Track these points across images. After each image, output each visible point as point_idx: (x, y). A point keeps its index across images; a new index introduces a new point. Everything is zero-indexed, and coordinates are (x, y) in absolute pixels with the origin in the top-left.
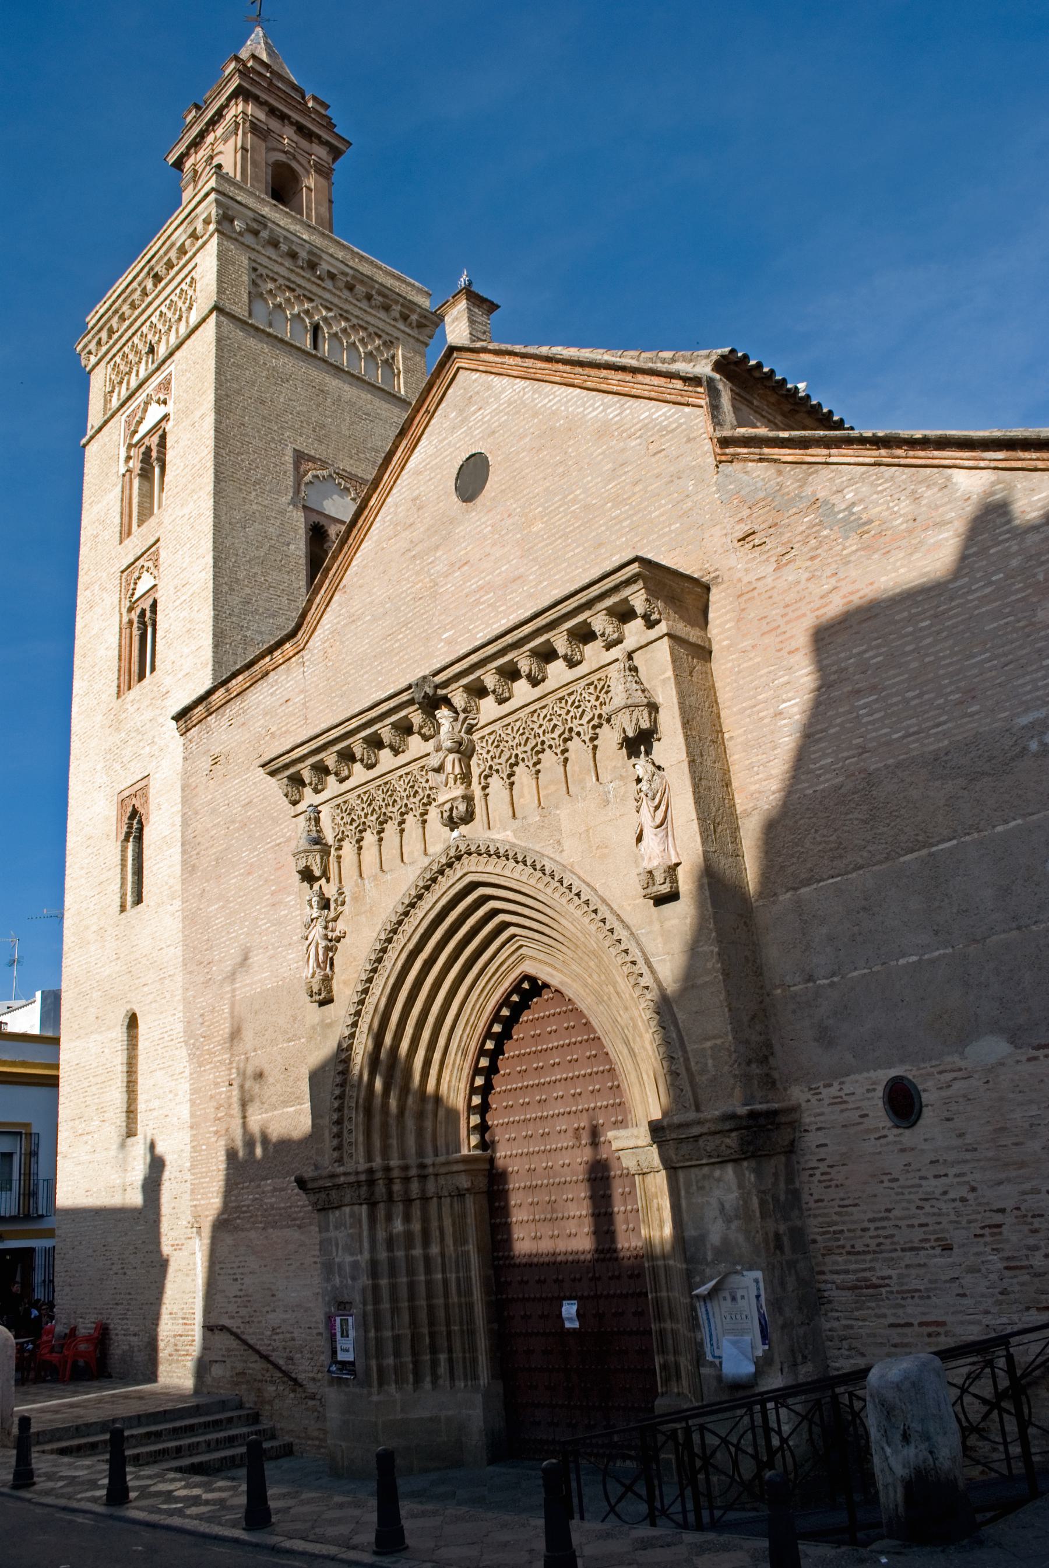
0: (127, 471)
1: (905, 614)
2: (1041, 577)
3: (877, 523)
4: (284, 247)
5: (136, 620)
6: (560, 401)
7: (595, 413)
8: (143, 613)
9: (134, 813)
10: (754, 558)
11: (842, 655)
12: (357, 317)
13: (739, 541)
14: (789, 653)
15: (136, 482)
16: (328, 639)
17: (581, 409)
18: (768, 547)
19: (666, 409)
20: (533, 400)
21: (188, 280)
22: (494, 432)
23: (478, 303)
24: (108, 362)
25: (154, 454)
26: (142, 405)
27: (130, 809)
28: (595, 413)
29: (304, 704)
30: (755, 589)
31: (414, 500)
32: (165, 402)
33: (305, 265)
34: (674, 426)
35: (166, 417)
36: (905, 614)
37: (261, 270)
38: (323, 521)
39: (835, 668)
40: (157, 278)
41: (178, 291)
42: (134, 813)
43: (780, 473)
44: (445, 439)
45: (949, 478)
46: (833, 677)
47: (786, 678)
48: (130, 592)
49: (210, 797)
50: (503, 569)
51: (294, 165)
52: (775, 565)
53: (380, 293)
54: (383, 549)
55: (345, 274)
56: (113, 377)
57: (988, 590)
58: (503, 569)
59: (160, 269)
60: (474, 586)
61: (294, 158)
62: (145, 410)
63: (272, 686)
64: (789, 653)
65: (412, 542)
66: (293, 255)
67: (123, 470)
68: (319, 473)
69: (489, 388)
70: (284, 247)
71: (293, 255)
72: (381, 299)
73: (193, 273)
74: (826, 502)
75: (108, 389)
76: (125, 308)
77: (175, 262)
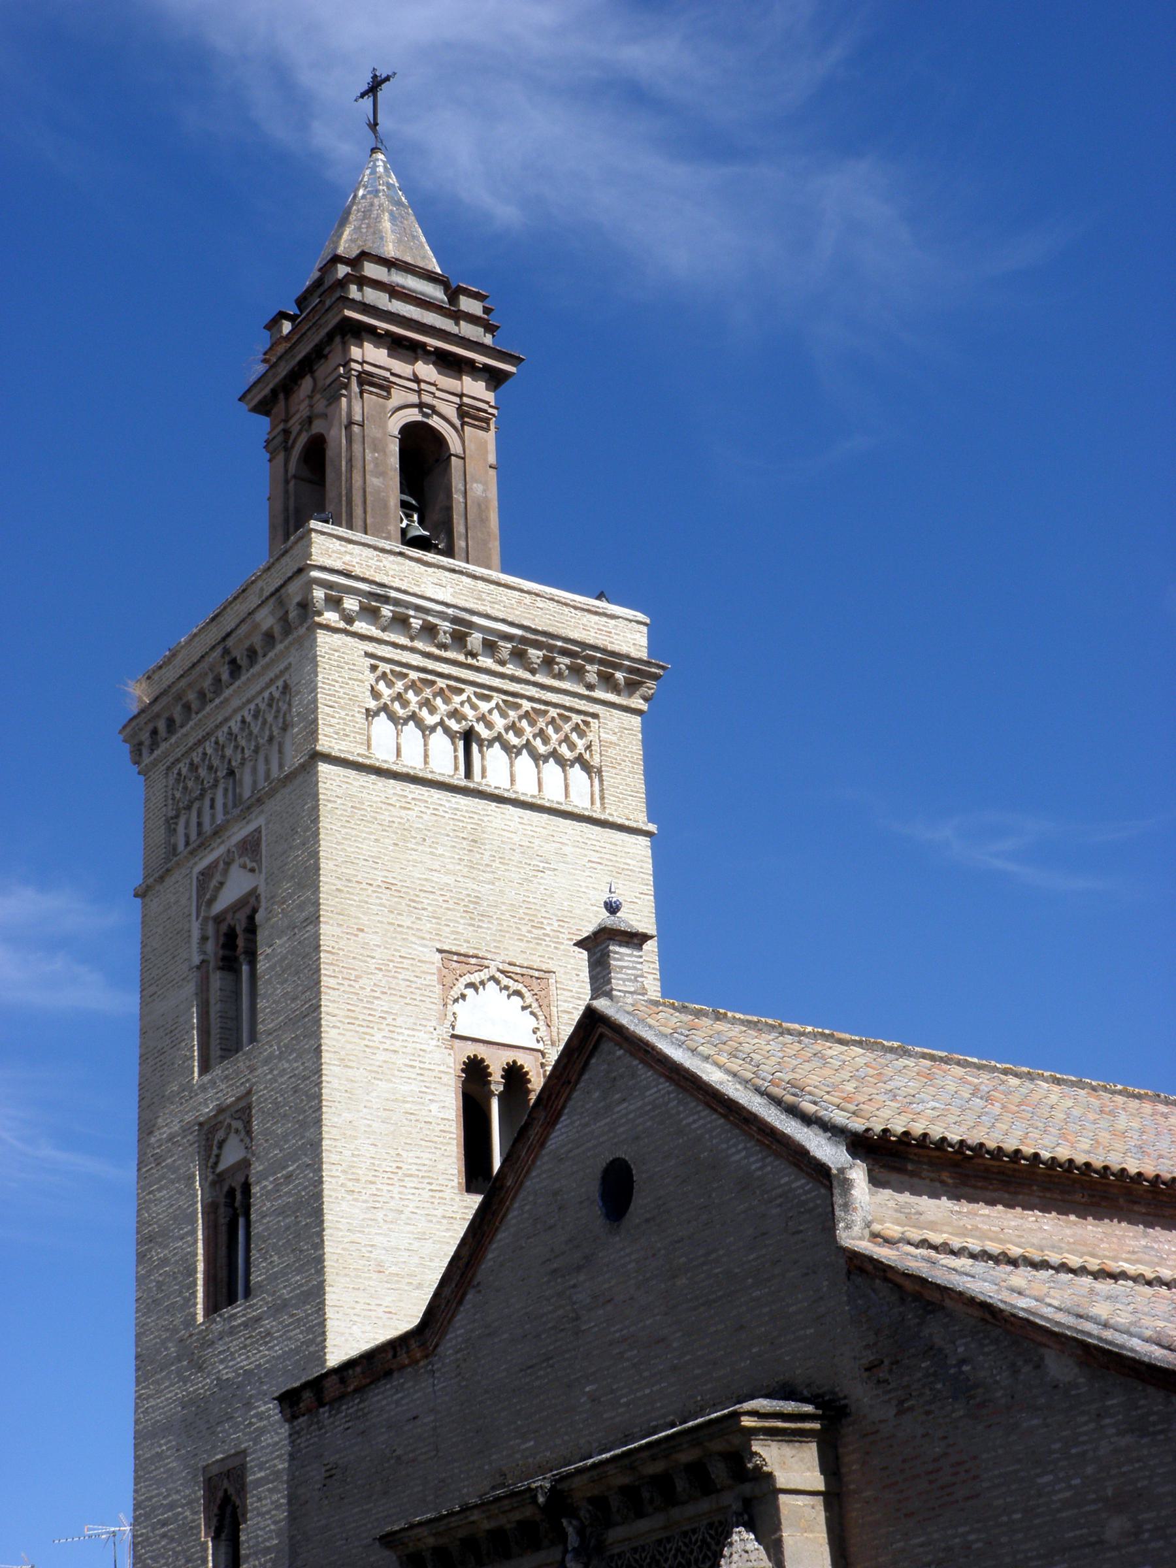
0: (203, 962)
1: (1001, 1501)
2: (1110, 1492)
3: (981, 1390)
4: (416, 623)
5: (222, 1200)
6: (704, 1125)
7: (737, 1157)
8: (231, 1193)
9: (226, 1500)
10: (878, 1395)
11: (949, 1532)
12: (531, 699)
13: (867, 1370)
14: (906, 1515)
15: (217, 980)
16: (461, 1350)
17: (724, 1146)
18: (890, 1387)
19: (803, 1181)
20: (679, 1113)
21: (280, 683)
22: (637, 1138)
23: (626, 939)
24: (169, 768)
25: (241, 942)
26: (221, 865)
27: (220, 1494)
28: (737, 1157)
29: (435, 1428)
30: (877, 1431)
31: (555, 1193)
32: (252, 870)
33: (449, 641)
34: (811, 1205)
35: (253, 893)
36: (1001, 1501)
37: (384, 667)
38: (482, 1052)
39: (943, 1545)
40: (235, 669)
41: (266, 694)
42: (226, 1500)
43: (902, 1300)
44: (586, 1125)
45: (1042, 1358)
46: (941, 1555)
47: (901, 1544)
48: (212, 1160)
49: (323, 1522)
50: (648, 1322)
51: (435, 422)
52: (894, 1412)
53: (565, 652)
54: (522, 1248)
55: (508, 637)
56: (178, 795)
57: (1068, 1494)
58: (648, 1322)
59: (239, 654)
60: (617, 1335)
61: (435, 411)
62: (226, 872)
63: (397, 1392)
64: (906, 1515)
65: (552, 1250)
66: (430, 631)
67: (196, 960)
68: (476, 978)
69: (633, 1075)
70: (416, 623)
71: (430, 631)
72: (567, 661)
73: (286, 676)
74: (940, 1350)
75: (172, 813)
76: (191, 696)
77: (260, 652)
